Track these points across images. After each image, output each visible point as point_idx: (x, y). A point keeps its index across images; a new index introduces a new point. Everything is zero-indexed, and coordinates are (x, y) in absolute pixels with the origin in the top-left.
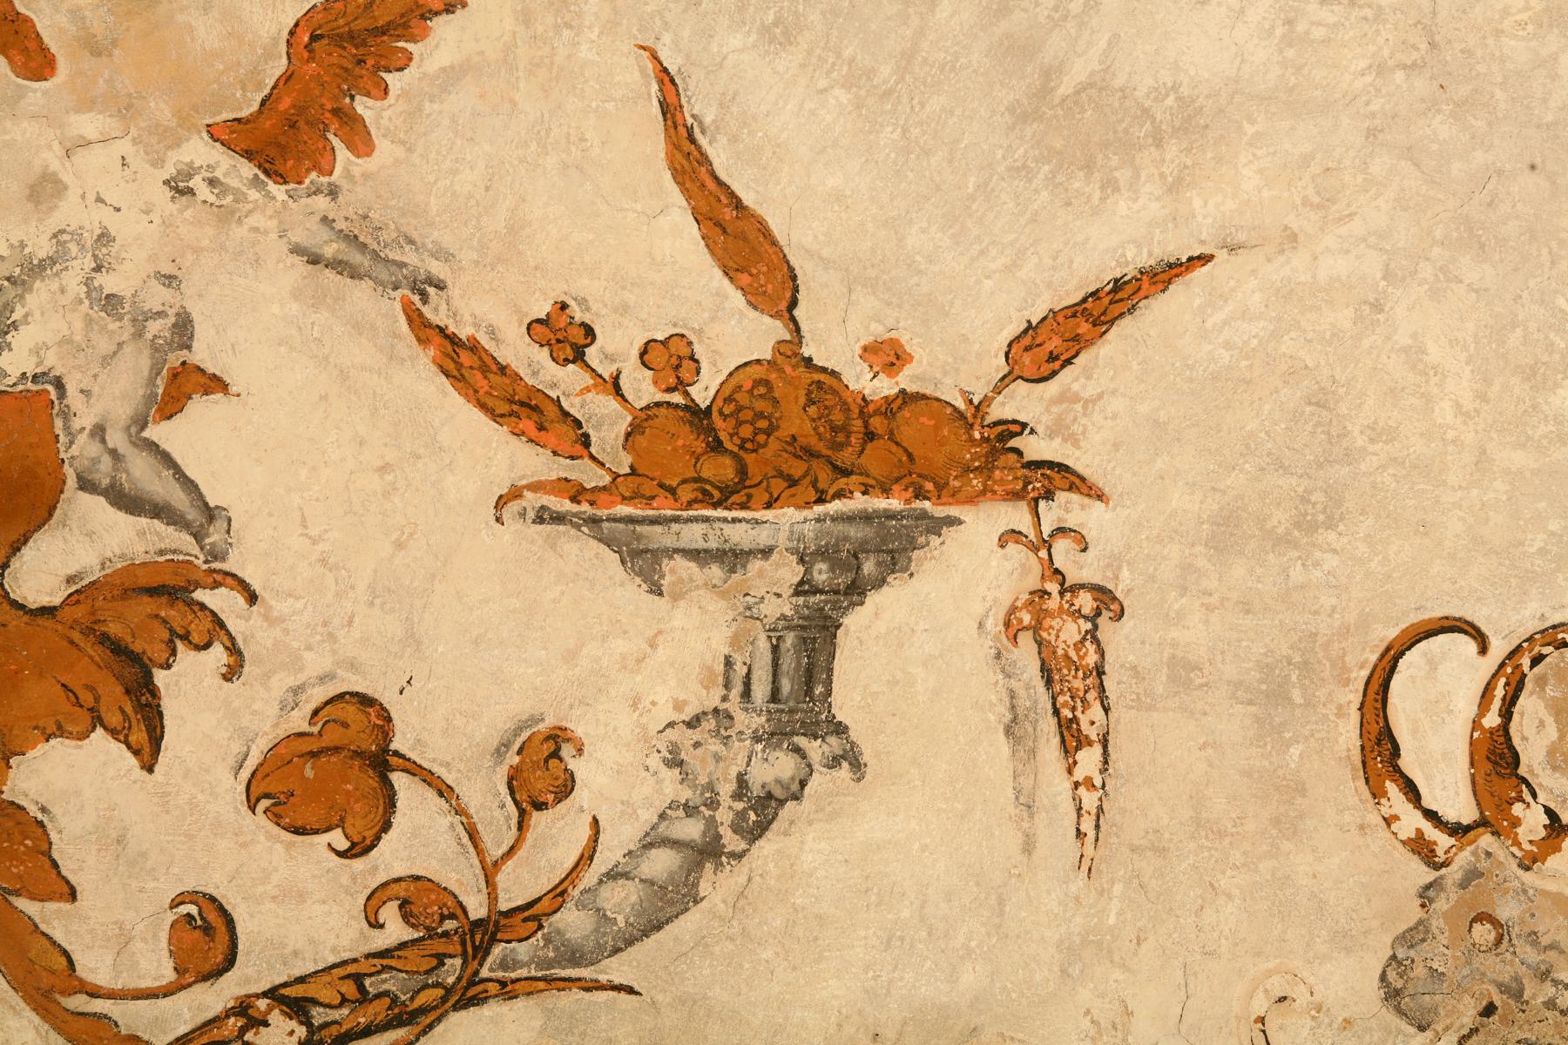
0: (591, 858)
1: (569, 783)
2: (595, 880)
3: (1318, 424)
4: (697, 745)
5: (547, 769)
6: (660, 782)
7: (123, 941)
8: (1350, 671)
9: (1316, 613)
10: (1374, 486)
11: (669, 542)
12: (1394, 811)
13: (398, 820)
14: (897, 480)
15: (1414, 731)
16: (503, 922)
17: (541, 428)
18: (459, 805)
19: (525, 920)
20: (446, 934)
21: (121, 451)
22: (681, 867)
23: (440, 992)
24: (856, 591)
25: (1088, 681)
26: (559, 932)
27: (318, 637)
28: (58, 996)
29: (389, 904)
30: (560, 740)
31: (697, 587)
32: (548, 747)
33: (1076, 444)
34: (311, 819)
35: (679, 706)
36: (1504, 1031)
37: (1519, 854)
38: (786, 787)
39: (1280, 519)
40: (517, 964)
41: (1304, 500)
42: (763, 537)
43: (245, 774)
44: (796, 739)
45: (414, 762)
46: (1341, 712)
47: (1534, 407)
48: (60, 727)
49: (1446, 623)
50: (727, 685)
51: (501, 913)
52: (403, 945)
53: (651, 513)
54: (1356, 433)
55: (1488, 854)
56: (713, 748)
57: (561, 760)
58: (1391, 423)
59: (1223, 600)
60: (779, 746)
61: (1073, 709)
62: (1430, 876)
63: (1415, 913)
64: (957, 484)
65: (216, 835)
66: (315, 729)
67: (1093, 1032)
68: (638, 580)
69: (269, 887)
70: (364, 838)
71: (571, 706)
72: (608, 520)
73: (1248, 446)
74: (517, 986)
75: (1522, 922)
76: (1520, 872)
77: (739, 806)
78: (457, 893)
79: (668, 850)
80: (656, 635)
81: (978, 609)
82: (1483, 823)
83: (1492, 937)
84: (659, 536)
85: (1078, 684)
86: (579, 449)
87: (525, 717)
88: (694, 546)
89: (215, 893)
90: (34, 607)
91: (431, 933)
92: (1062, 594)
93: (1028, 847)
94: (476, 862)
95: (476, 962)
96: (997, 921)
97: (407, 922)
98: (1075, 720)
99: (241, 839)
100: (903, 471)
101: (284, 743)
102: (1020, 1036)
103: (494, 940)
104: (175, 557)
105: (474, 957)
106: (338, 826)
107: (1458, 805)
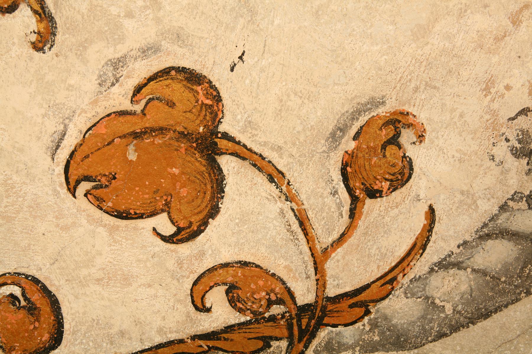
0: (424, 248)
1: (406, 171)
2: (426, 269)
5: (384, 156)
6: (505, 172)
13: (225, 205)
16: (330, 307)
18: (289, 191)
19: (351, 306)
20: (273, 319)
22: (517, 259)
26: (386, 318)
29: (215, 289)
30: (400, 125)
32: (386, 133)
43: (63, 155)
45: (245, 146)
51: (329, 299)
52: (229, 329)
57: (400, 147)
65: (35, 217)
66: (138, 108)
69: (93, 270)
70: (191, 223)
71: (416, 89)
78: (285, 279)
79: (505, 242)
80: (521, 10)
87: (363, 100)
94: (305, 248)
95: (301, 346)
97: (234, 307)
101: (104, 122)
103: (320, 324)
105: (300, 341)
106: (163, 211)
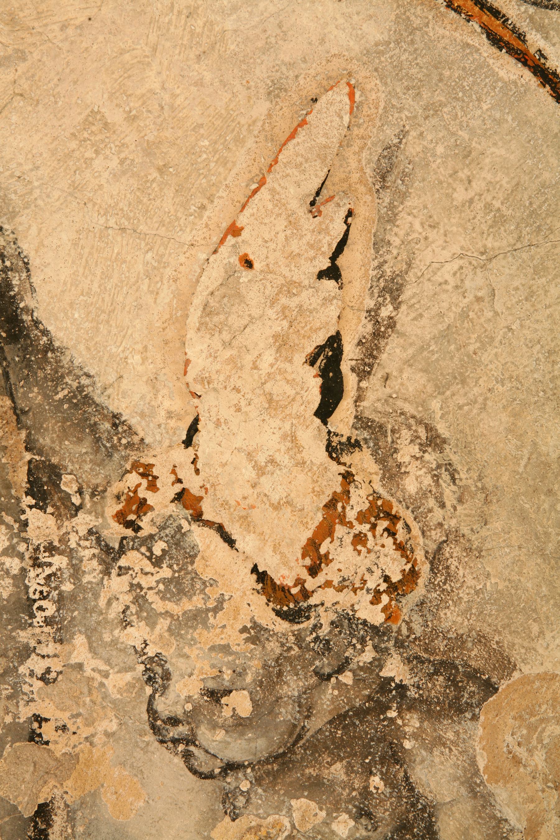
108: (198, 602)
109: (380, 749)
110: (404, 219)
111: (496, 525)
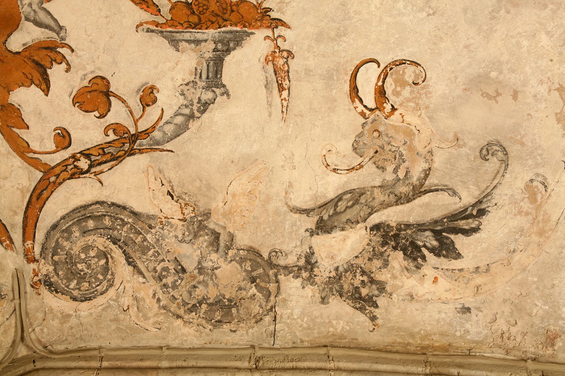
0: (162, 118)
2: (163, 124)
3: (342, 10)
4: (188, 90)
6: (179, 99)
7: (42, 140)
8: (348, 72)
9: (340, 57)
10: (355, 26)
11: (181, 38)
12: (356, 106)
13: (111, 109)
14: (239, 23)
15: (362, 86)
16: (139, 134)
17: (148, 7)
19: (145, 134)
20: (125, 138)
21: (36, 10)
23: (124, 152)
24: (228, 51)
25: (285, 74)
26: (154, 137)
27: (90, 61)
28: (25, 153)
31: (188, 50)
32: (150, 91)
33: (284, 14)
34: (89, 108)
35: (183, 80)
36: (380, 157)
37: (385, 115)
38: (210, 100)
39: (333, 34)
40: (143, 145)
41: (339, 29)
42: (205, 37)
43: (72, 97)
44: (213, 88)
46: (345, 82)
47: (393, 7)
48: (23, 84)
49: (371, 60)
50: (196, 75)
51: (139, 132)
52: (114, 141)
53: (176, 30)
54: (352, 13)
55: (378, 116)
56: (192, 91)
57: (153, 94)
58: (360, 10)
59: (318, 54)
60: (209, 90)
61: (282, 81)
62: (364, 121)
63: (361, 130)
64: (254, 24)
66: (90, 85)
67: (285, 160)
68: (173, 48)
71: (156, 80)
72: (165, 32)
73: (325, 15)
74: (143, 150)
75: (385, 131)
76: (385, 120)
77: (199, 105)
81: (259, 56)
82: (377, 108)
83: (378, 135)
84: (178, 36)
85: (283, 75)
86: (158, 13)
87: (144, 83)
88: (187, 39)
89: (65, 127)
90: (14, 52)
91: (121, 137)
92: (279, 52)
93: (270, 115)
94: (132, 120)
96: (262, 133)
98: (282, 84)
99: (72, 114)
100: (241, 20)
102: (267, 161)
103: (137, 139)
104: (52, 39)
107: (371, 104)
108: (175, 227)
109: (204, 227)
110: (166, 174)
111: (199, 197)
